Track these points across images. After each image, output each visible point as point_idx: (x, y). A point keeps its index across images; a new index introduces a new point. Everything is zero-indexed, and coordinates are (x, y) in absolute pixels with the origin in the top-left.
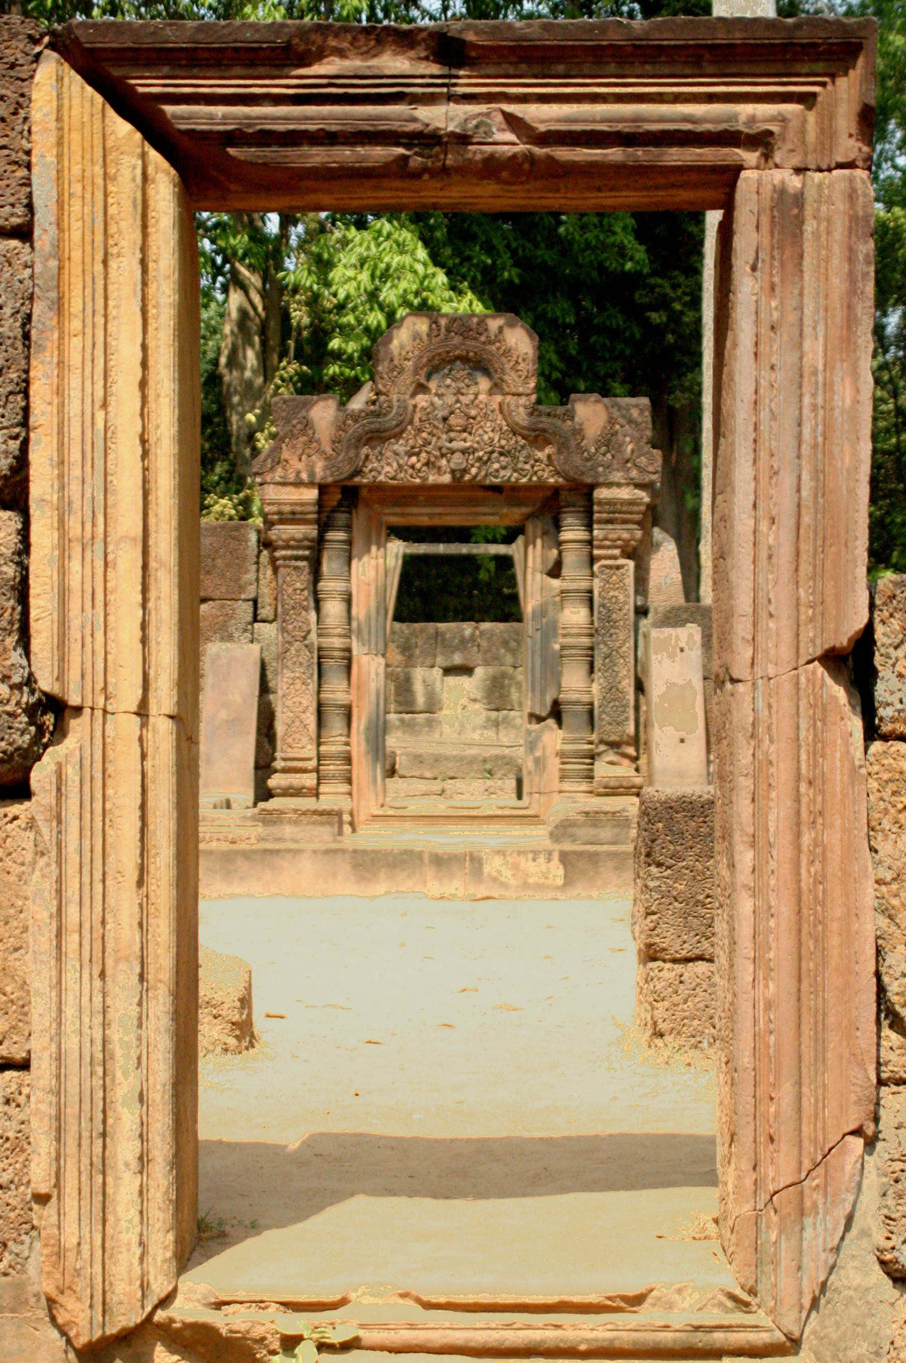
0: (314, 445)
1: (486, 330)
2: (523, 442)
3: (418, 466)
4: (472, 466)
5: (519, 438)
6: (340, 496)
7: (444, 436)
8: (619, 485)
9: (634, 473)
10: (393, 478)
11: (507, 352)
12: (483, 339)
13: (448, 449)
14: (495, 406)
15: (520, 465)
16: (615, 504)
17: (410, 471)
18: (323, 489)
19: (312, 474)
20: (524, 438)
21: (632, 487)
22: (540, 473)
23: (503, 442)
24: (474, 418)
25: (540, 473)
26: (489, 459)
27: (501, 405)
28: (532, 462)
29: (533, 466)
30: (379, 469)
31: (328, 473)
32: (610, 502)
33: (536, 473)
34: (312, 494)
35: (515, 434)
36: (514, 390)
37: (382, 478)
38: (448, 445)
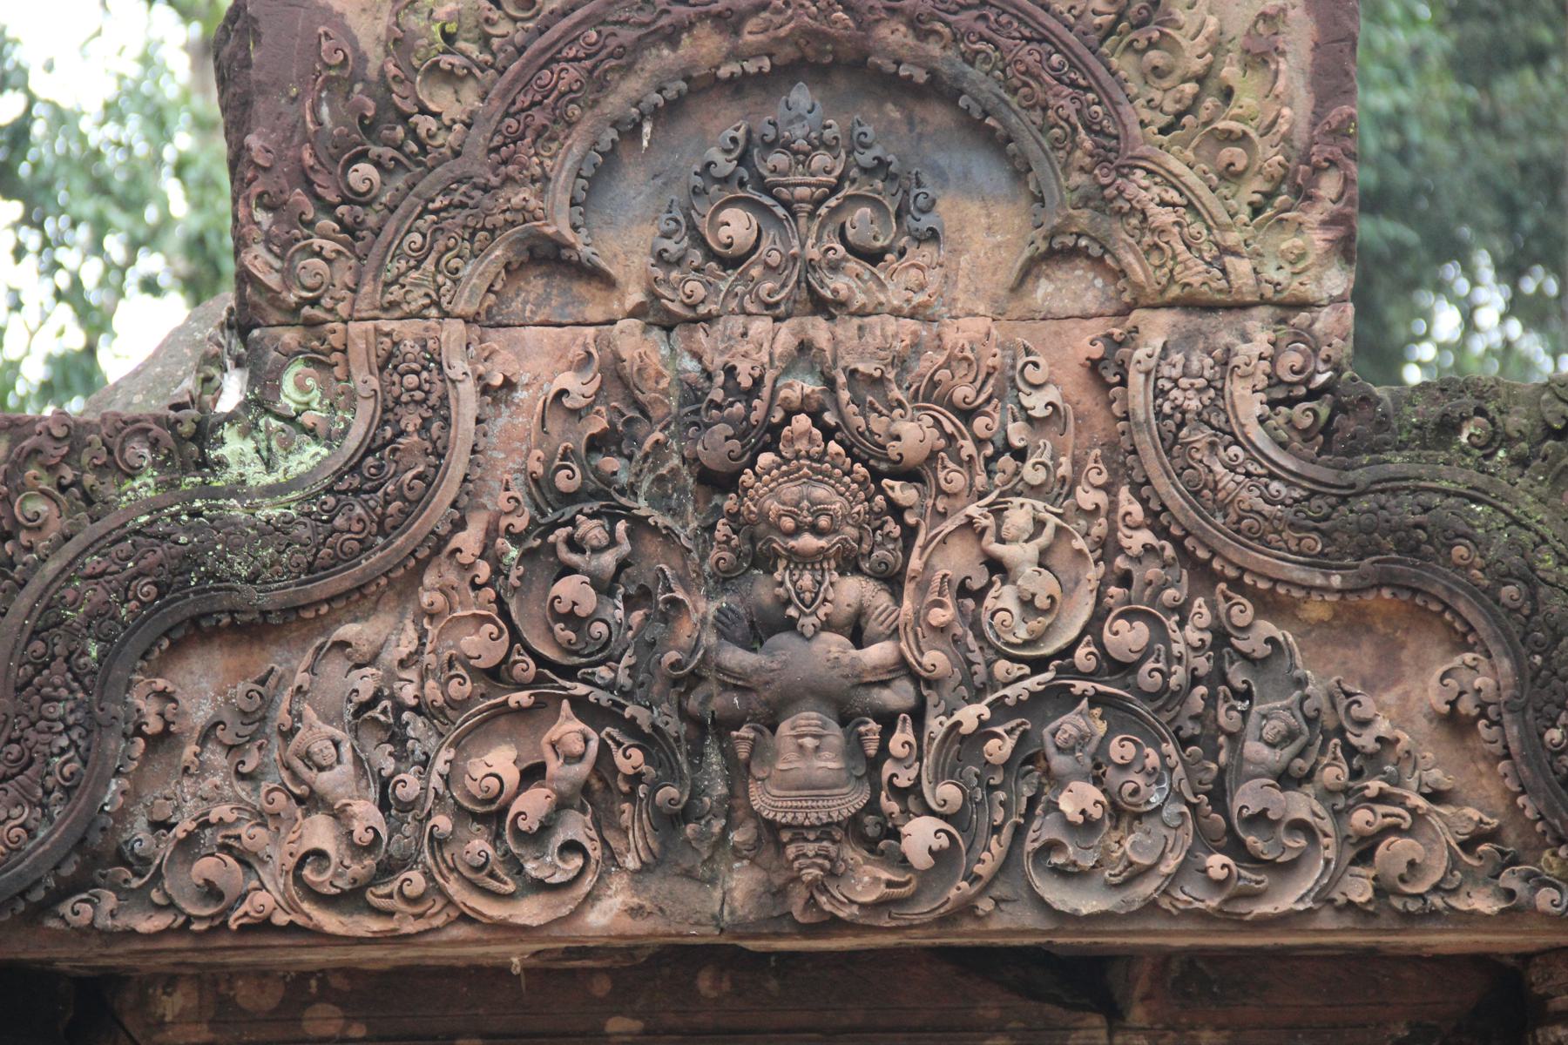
3: (533, 804)
4: (911, 796)
5: (1242, 612)
7: (704, 607)
10: (351, 899)
13: (740, 683)
15: (1248, 797)
22: (1396, 851)
23: (1127, 637)
24: (911, 475)
26: (1028, 757)
28: (1334, 773)
29: (1342, 800)
33: (1364, 850)
35: (1204, 575)
36: (1195, 274)
37: (267, 898)
38: (736, 657)
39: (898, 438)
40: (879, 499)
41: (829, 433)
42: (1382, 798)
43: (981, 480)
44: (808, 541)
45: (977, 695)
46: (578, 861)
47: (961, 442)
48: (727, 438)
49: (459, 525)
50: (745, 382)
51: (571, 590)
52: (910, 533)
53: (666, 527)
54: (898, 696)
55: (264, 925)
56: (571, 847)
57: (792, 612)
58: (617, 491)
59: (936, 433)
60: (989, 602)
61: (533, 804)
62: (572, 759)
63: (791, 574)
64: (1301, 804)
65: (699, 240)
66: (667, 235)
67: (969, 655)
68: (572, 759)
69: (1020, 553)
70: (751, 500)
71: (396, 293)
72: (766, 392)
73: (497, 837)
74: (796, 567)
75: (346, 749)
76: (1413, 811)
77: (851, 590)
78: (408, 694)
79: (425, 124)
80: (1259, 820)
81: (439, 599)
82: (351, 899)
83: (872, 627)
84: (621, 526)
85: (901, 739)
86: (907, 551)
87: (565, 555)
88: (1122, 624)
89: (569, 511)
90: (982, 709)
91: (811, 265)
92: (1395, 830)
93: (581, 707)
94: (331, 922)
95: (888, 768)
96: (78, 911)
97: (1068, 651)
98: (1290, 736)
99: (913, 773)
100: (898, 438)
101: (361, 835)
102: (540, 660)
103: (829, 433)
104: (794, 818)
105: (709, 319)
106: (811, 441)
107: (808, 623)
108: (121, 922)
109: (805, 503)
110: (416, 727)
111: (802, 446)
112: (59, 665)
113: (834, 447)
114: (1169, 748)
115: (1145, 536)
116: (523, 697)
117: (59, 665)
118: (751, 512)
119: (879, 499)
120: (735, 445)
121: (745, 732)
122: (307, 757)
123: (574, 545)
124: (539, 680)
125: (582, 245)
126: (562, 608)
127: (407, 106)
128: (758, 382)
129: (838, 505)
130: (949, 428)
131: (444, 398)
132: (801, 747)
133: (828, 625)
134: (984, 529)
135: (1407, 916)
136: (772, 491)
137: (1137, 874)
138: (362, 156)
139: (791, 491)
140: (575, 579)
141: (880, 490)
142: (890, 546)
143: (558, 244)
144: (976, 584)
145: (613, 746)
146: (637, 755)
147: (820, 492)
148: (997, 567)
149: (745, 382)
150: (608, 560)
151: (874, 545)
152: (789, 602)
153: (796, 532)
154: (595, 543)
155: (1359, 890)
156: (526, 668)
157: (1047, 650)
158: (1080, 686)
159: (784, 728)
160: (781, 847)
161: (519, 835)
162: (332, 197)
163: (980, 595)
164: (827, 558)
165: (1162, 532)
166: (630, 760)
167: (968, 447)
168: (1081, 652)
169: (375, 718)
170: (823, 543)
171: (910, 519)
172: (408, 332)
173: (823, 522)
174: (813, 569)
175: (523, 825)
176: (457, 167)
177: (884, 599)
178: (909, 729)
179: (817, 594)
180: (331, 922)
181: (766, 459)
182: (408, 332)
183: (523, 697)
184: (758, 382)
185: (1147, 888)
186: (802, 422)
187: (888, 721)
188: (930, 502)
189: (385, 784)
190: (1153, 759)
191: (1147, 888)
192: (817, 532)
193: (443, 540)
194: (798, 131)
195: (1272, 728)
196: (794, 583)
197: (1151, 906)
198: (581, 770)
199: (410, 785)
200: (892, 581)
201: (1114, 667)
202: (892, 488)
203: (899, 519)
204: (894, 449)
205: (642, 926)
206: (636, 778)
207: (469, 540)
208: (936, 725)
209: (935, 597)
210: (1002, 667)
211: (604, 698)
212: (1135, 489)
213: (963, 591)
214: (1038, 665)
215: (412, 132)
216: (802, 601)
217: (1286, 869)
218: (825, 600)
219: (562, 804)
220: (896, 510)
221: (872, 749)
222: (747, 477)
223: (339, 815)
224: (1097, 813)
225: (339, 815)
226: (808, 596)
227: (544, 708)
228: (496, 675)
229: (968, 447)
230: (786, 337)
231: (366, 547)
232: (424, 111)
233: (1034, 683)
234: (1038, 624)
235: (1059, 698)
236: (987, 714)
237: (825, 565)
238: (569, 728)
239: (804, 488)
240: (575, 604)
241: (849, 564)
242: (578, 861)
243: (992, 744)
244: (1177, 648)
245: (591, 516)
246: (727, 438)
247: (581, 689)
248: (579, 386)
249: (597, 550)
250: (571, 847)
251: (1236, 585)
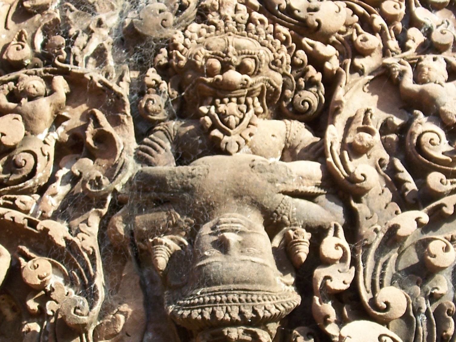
39: (316, 10)
40: (301, 54)
43: (393, 44)
47: (374, 15)
48: (161, 11)
52: (331, 81)
53: (101, 82)
57: (216, 133)
58: (60, 60)
59: (351, 12)
63: (217, 107)
67: (400, 176)
70: (181, 52)
74: (222, 102)
99: (349, 277)
100: (316, 10)
104: (213, 313)
106: (236, 10)
109: (231, 48)
118: (178, 59)
119: (301, 54)
130: (361, 10)
134: (402, 73)
141: (300, 46)
142: (314, 89)
145: (22, 260)
151: (298, 89)
152: (215, 126)
154: (33, 91)
164: (250, 94)
167: (378, 21)
170: (246, 76)
171: (333, 65)
174: (239, 102)
178: (341, 232)
179: (241, 120)
188: (348, 61)
192: (242, 69)
196: (219, 114)
200: (317, 122)
202: (312, 46)
203: (320, 68)
204: (312, 19)
209: (361, 125)
211: (20, 218)
216: (227, 124)
218: (250, 123)
226: (233, 120)
236: (425, 219)
237: (250, 100)
239: (230, 39)
240: (3, 135)
245: (29, 74)
246: (161, 11)
249: (31, 98)
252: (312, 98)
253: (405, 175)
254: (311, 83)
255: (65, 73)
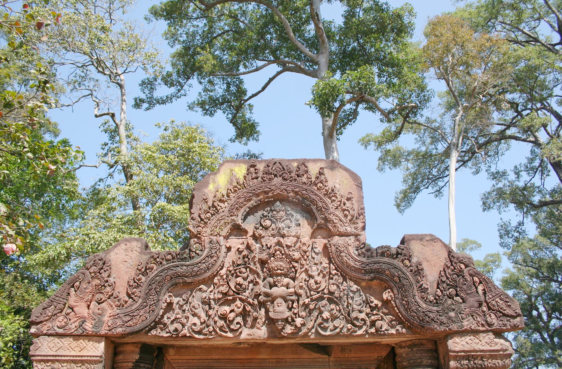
0: (108, 289)
1: (307, 172)
2: (355, 287)
5: (352, 283)
6: (137, 357)
8: (475, 332)
9: (493, 319)
11: (331, 194)
12: (304, 179)
13: (267, 295)
14: (319, 249)
15: (354, 315)
16: (475, 358)
17: (221, 323)
18: (115, 345)
19: (98, 323)
20: (356, 283)
21: (491, 336)
24: (297, 262)
25: (378, 324)
27: (325, 247)
28: (368, 310)
30: (184, 321)
31: (119, 322)
32: (469, 356)
34: (98, 349)
41: (283, 255)
42: (376, 314)
44: (279, 271)
45: (308, 297)
46: (239, 326)
49: (221, 269)
50: (269, 246)
51: (240, 280)
52: (296, 271)
54: (294, 298)
55: (185, 336)
56: (238, 323)
60: (310, 282)
61: (232, 316)
62: (239, 308)
64: (363, 316)
65: (261, 225)
66: (256, 224)
68: (239, 308)
69: (315, 273)
71: (213, 232)
72: (272, 248)
73: (226, 322)
75: (201, 307)
76: (381, 316)
77: (286, 280)
78: (212, 297)
79: (218, 208)
80: (357, 319)
81: (217, 281)
82: (199, 332)
83: (290, 286)
84: (248, 269)
85: (295, 305)
86: (296, 274)
87: (238, 274)
88: (332, 286)
89: (239, 267)
90: (309, 300)
91: (280, 228)
92: (378, 320)
93: (241, 299)
94: (197, 336)
95: (293, 310)
96: (154, 332)
97: (323, 290)
98: (360, 304)
101: (202, 321)
102: (234, 292)
103: (283, 255)
105: (264, 237)
107: (279, 285)
108: (161, 335)
110: (212, 302)
111: (278, 256)
112: (153, 289)
113: (283, 256)
114: (340, 306)
115: (335, 271)
116: (231, 298)
117: (153, 289)
120: (267, 256)
121: (268, 303)
122: (193, 307)
123: (240, 272)
124: (233, 295)
125: (243, 226)
126: (238, 282)
127: (216, 205)
128: (271, 246)
129: (284, 266)
131: (220, 248)
132: (278, 306)
133: (283, 286)
135: (381, 335)
136: (274, 264)
137: (336, 328)
138: (209, 212)
139: (276, 263)
140: (240, 278)
143: (239, 226)
144: (308, 279)
146: (250, 307)
147: (281, 263)
148: (311, 277)
149: (269, 246)
150: (245, 275)
153: (277, 270)
155: (373, 330)
156: (231, 293)
157: (319, 290)
158: (325, 296)
159: (275, 302)
160: (274, 323)
161: (229, 321)
162: (203, 218)
163: (308, 281)
165: (338, 271)
166: (249, 308)
167: (306, 257)
168: (325, 290)
169: (206, 302)
172: (214, 238)
173: (282, 268)
175: (230, 319)
176: (223, 214)
177: (292, 282)
180: (197, 336)
181: (272, 258)
182: (214, 238)
183: (231, 298)
184: (271, 246)
185: (338, 330)
186: (278, 252)
187: (293, 302)
189: (207, 312)
190: (338, 308)
191: (338, 330)
193: (218, 272)
194: (278, 208)
195: (358, 303)
197: (338, 333)
198: (241, 309)
199: (211, 312)
200: (294, 279)
201: (331, 293)
204: (294, 257)
205: (250, 337)
206: (250, 311)
207: (223, 272)
208: (301, 303)
210: (312, 293)
211: (244, 298)
212: (333, 264)
213: (305, 281)
214: (318, 292)
215: (216, 209)
217: (360, 327)
219: (237, 316)
220: (294, 267)
221: (290, 306)
222: (269, 261)
223: (199, 318)
224: (329, 317)
225: (199, 318)
227: (234, 300)
228: (225, 294)
229: (306, 257)
230: (275, 240)
231: (205, 272)
232: (219, 206)
233: (317, 295)
234: (318, 286)
235: (321, 298)
238: (238, 302)
241: (286, 276)
242: (239, 326)
243: (311, 305)
244: (341, 290)
247: (240, 296)
248: (242, 247)
249: (244, 273)
250: (238, 323)
251: (351, 279)
252: (292, 274)
253: (308, 291)
254: (293, 272)
255: (249, 267)
